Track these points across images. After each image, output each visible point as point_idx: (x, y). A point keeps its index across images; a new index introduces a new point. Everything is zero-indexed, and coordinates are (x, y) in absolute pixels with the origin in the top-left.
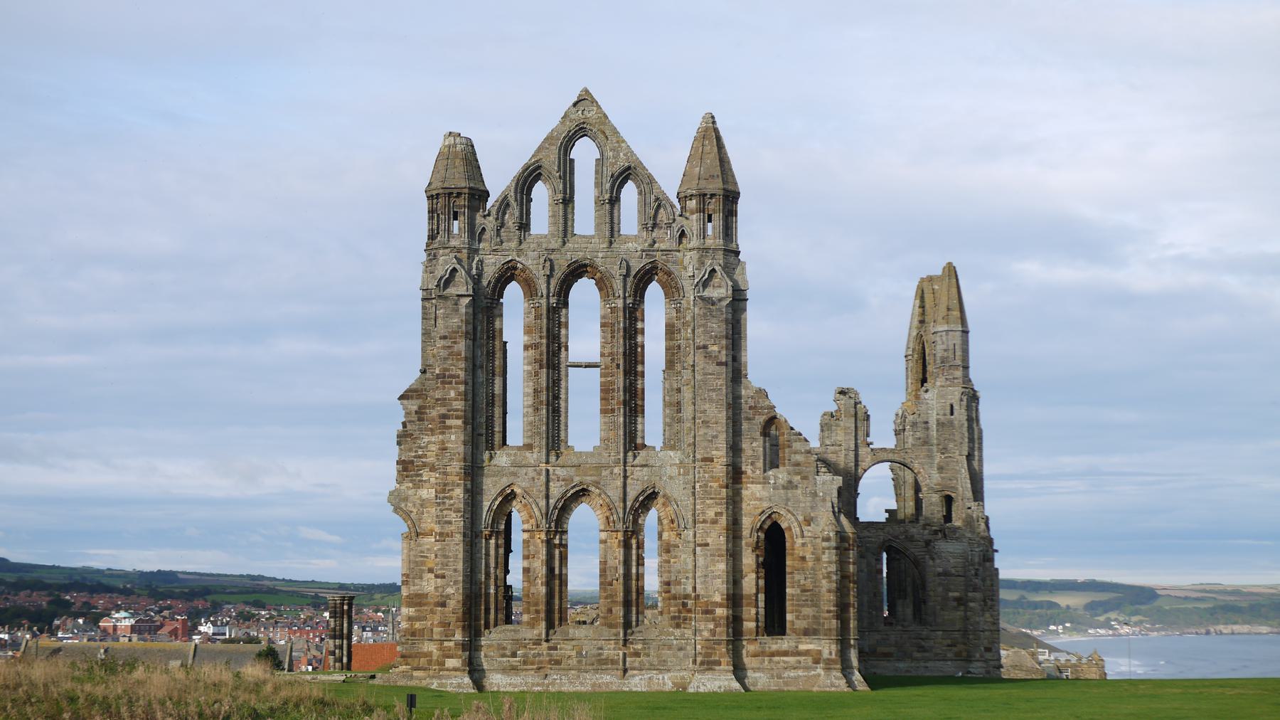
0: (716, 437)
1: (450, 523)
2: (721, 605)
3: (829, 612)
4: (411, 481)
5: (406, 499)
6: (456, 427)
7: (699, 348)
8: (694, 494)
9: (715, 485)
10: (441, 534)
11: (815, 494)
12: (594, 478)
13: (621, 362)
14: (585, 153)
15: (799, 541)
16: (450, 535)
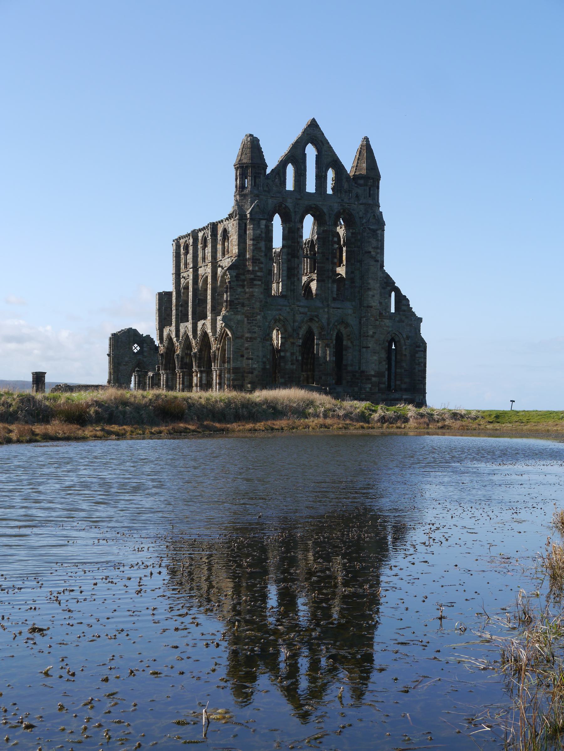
0: (373, 296)
1: (255, 332)
2: (374, 376)
3: (419, 380)
4: (233, 311)
5: (230, 320)
6: (259, 285)
7: (366, 252)
8: (360, 323)
9: (373, 319)
10: (251, 338)
11: (411, 325)
12: (316, 313)
13: (330, 257)
14: (311, 152)
15: (404, 347)
16: (255, 339)
